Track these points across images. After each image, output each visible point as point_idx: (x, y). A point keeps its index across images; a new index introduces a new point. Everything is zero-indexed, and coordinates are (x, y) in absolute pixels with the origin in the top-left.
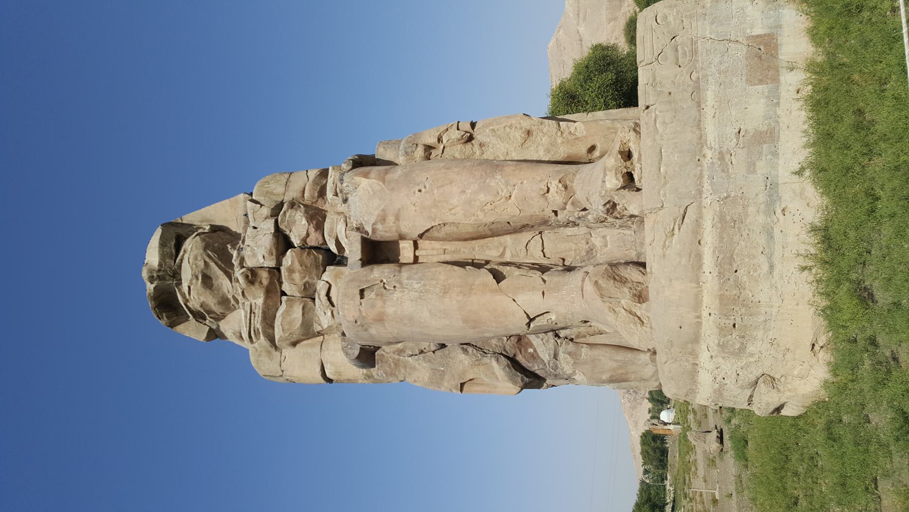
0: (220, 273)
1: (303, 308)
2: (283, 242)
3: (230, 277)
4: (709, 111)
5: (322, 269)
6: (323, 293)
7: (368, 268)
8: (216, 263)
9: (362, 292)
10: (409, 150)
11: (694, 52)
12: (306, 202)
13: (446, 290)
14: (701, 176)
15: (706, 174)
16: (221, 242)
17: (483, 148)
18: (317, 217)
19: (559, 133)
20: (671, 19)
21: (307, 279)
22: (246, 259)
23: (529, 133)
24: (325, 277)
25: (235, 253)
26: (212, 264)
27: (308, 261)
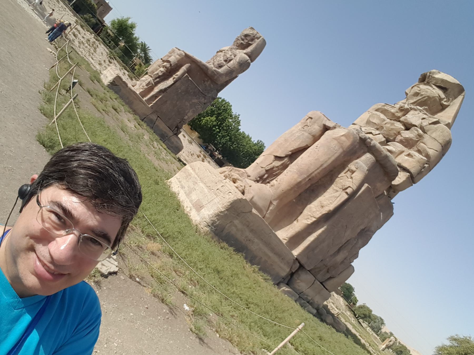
0: (415, 100)
1: (375, 123)
2: (408, 127)
3: (413, 104)
4: (204, 187)
5: (386, 137)
6: (373, 132)
7: (322, 126)
8: (420, 99)
9: (311, 118)
10: (357, 165)
11: (216, 194)
12: (419, 142)
13: (286, 140)
14: (198, 177)
15: (198, 178)
16: (434, 107)
17: (335, 191)
18: (408, 143)
19: (312, 215)
20: (227, 196)
21: (385, 129)
22: (415, 112)
23: (322, 207)
24: (381, 136)
25: (421, 108)
26: (420, 98)
27: (392, 133)
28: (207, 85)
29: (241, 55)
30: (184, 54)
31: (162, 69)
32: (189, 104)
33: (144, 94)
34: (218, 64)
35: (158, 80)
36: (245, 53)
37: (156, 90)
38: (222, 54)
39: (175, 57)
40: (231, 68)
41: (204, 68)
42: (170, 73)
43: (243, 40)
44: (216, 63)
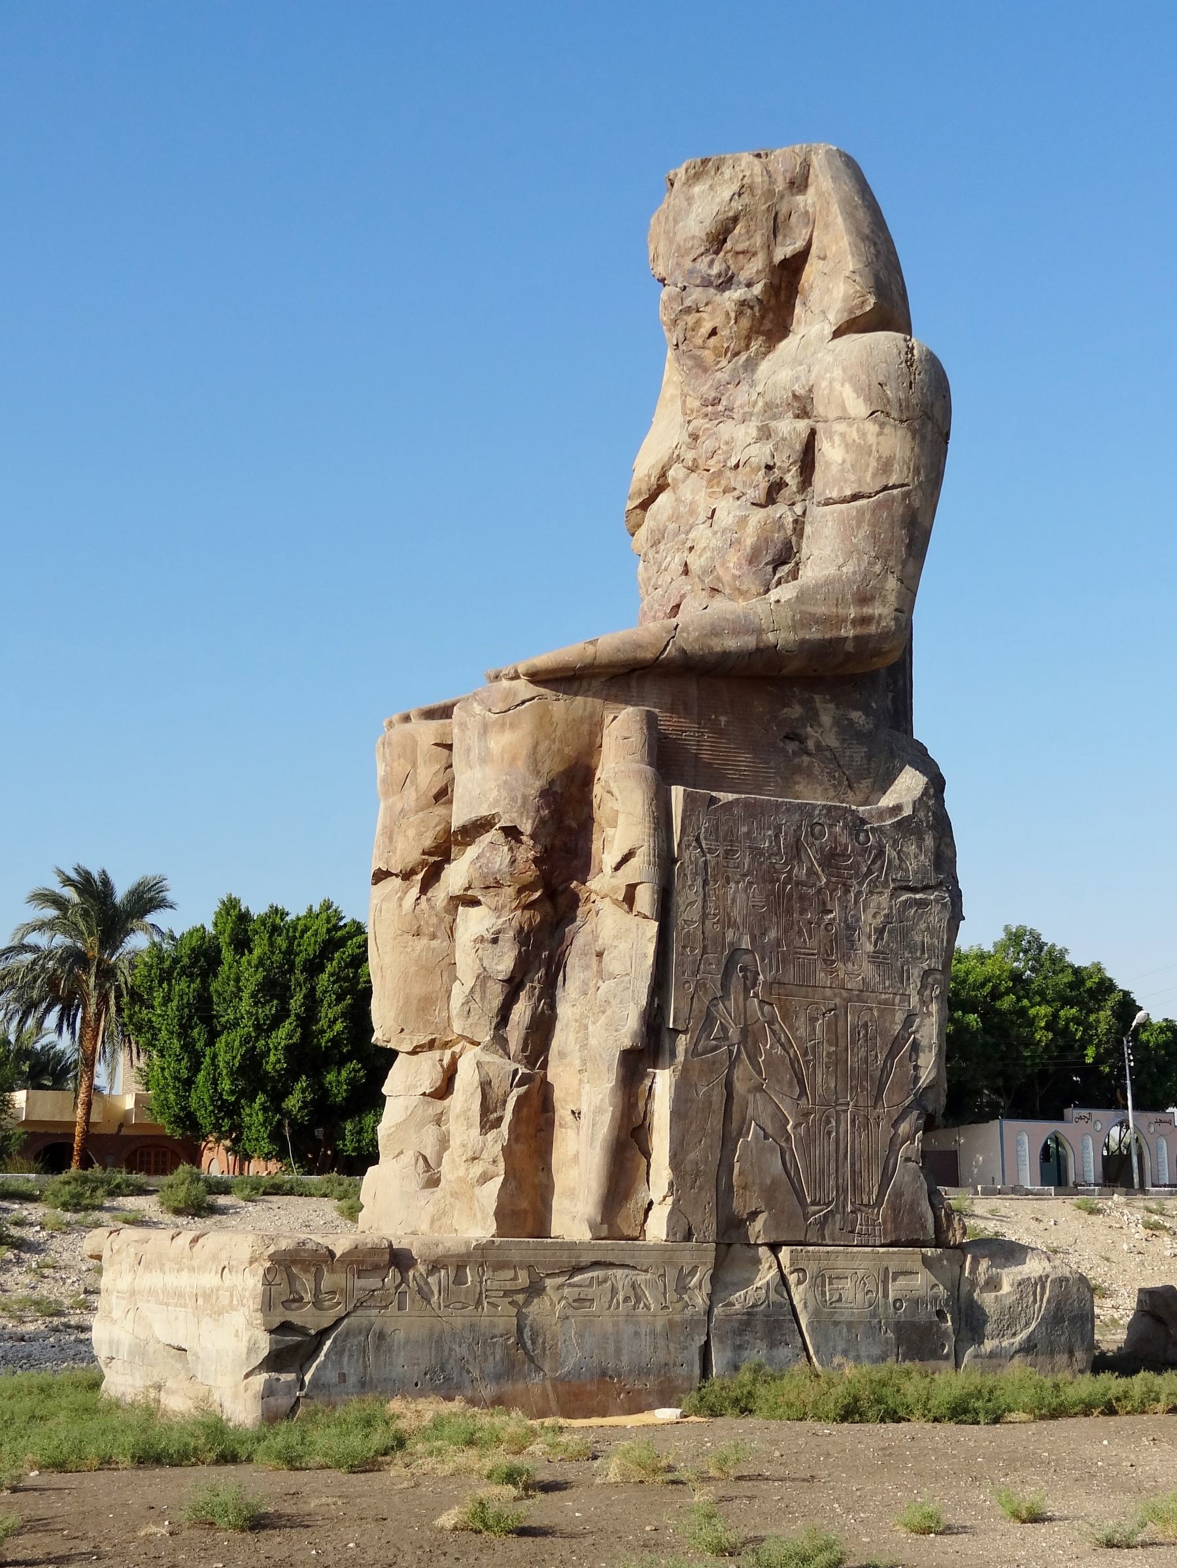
28: (831, 740)
29: (827, 362)
30: (524, 689)
31: (474, 923)
32: (867, 969)
33: (526, 1200)
34: (753, 558)
35: (521, 1012)
36: (837, 334)
37: (584, 1090)
38: (689, 491)
39: (484, 760)
40: (870, 483)
41: (731, 644)
42: (551, 894)
43: (727, 282)
44: (733, 564)
